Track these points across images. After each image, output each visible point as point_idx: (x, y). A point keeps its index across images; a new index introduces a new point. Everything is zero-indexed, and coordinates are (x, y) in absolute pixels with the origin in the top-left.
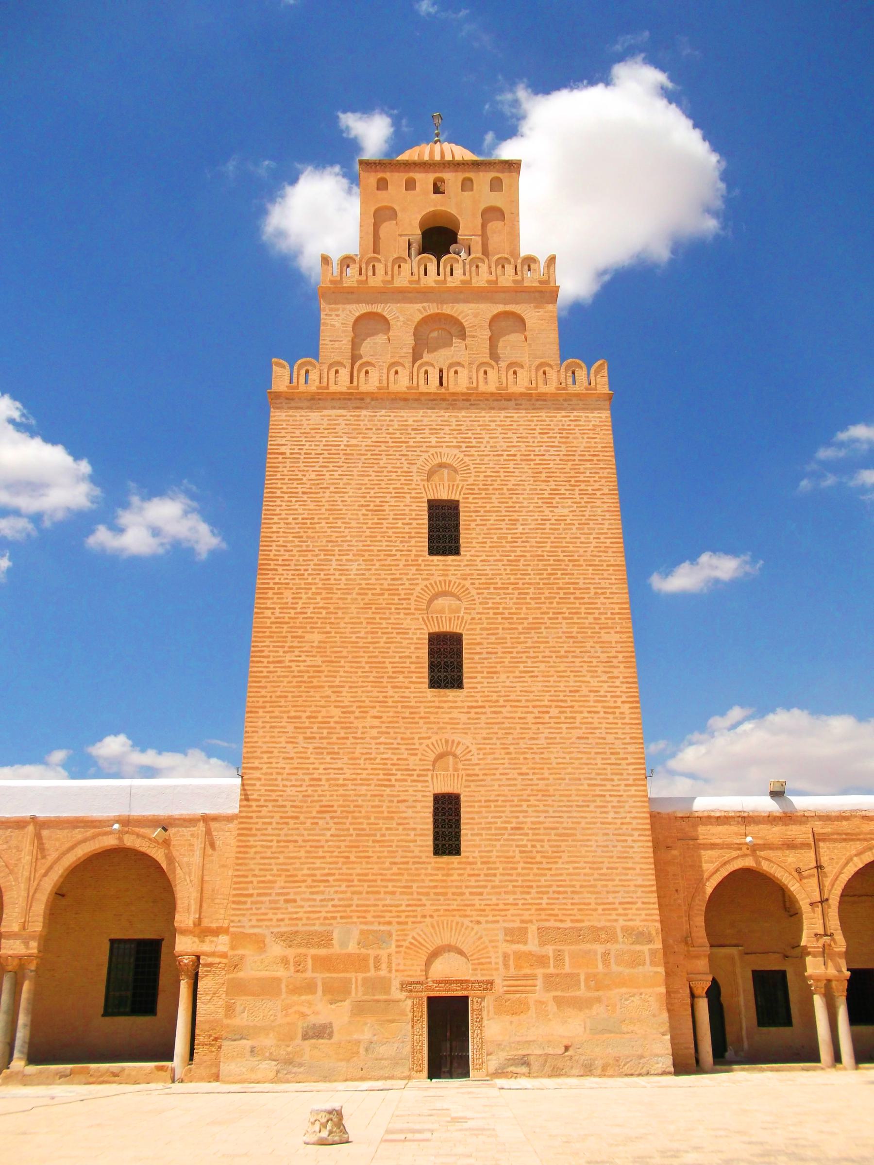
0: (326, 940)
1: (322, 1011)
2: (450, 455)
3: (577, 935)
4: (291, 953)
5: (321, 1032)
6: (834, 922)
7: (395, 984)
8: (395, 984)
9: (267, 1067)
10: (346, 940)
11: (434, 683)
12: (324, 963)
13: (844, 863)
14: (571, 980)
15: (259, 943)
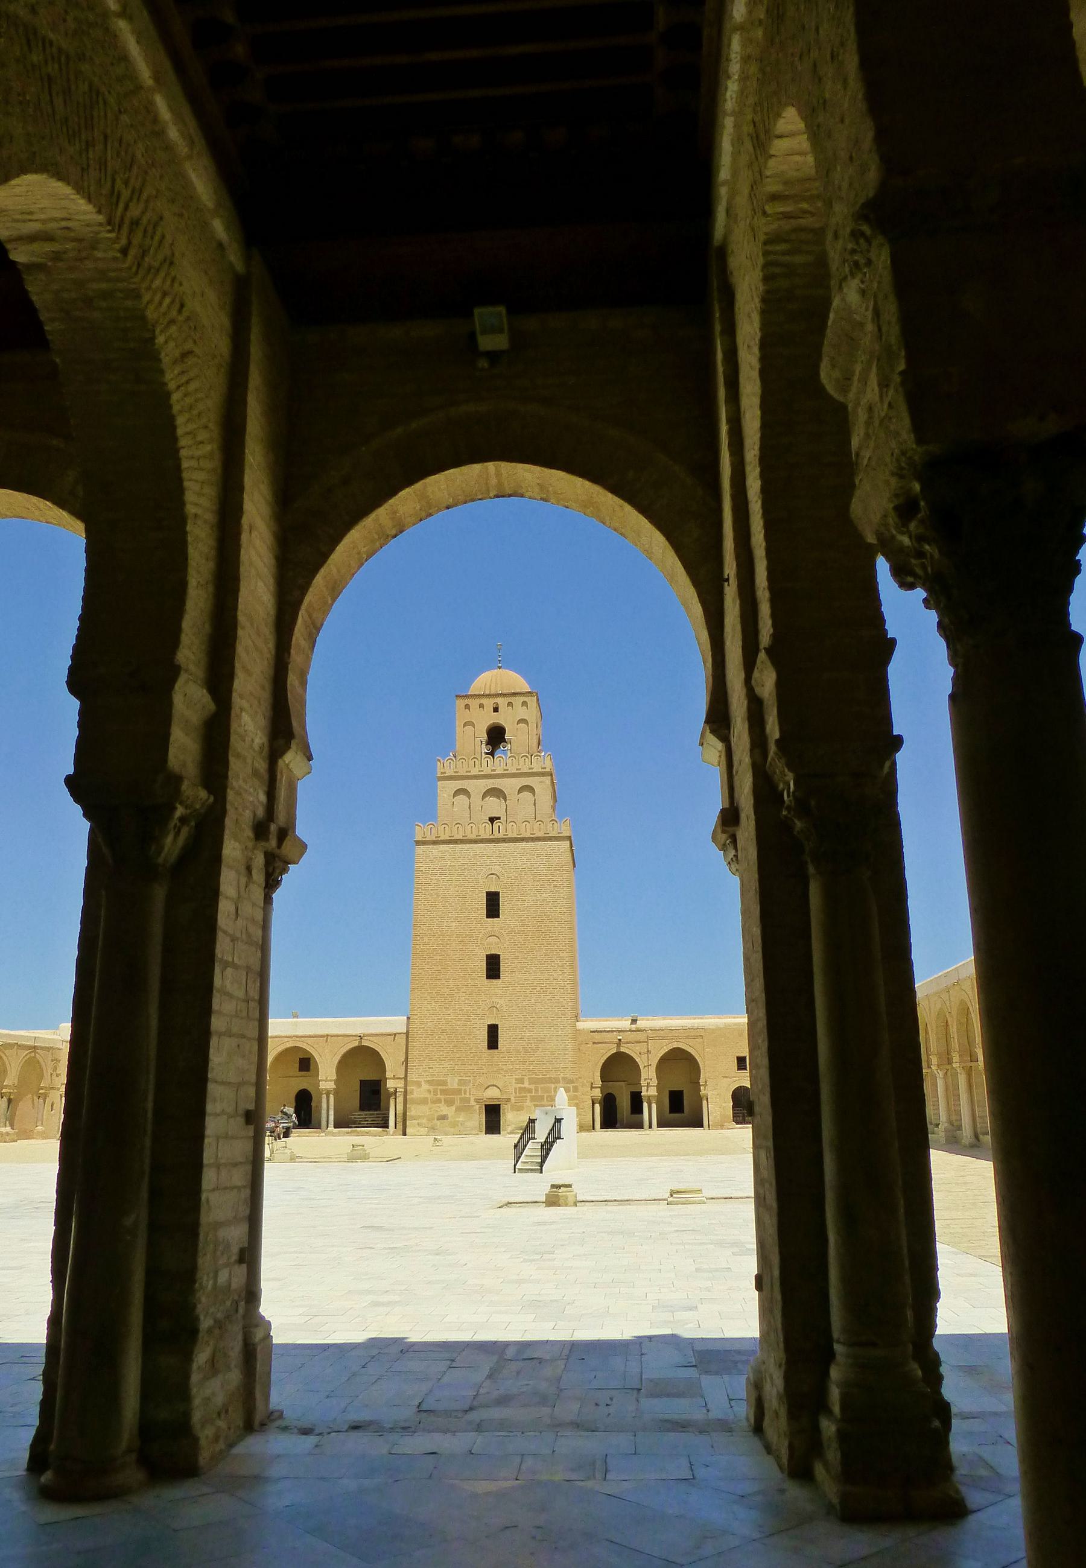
0: (444, 1083)
1: (444, 1110)
2: (496, 869)
3: (543, 1081)
4: (431, 1088)
5: (443, 1118)
6: (653, 1074)
7: (472, 1100)
8: (472, 1100)
9: (424, 1130)
10: (453, 1083)
11: (489, 977)
12: (443, 1092)
13: (660, 1050)
14: (542, 1098)
15: (419, 1084)
